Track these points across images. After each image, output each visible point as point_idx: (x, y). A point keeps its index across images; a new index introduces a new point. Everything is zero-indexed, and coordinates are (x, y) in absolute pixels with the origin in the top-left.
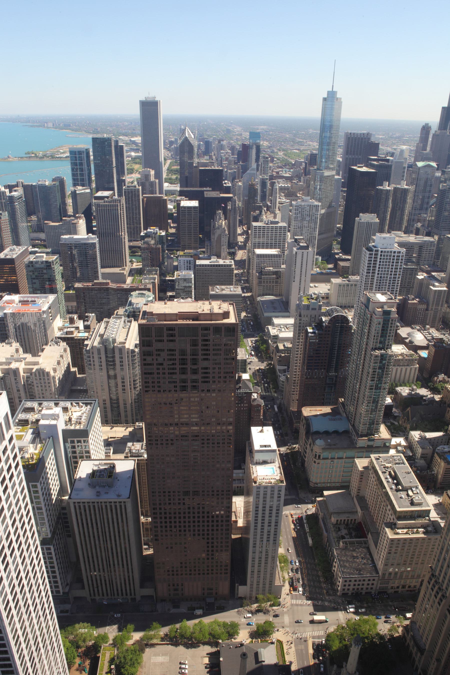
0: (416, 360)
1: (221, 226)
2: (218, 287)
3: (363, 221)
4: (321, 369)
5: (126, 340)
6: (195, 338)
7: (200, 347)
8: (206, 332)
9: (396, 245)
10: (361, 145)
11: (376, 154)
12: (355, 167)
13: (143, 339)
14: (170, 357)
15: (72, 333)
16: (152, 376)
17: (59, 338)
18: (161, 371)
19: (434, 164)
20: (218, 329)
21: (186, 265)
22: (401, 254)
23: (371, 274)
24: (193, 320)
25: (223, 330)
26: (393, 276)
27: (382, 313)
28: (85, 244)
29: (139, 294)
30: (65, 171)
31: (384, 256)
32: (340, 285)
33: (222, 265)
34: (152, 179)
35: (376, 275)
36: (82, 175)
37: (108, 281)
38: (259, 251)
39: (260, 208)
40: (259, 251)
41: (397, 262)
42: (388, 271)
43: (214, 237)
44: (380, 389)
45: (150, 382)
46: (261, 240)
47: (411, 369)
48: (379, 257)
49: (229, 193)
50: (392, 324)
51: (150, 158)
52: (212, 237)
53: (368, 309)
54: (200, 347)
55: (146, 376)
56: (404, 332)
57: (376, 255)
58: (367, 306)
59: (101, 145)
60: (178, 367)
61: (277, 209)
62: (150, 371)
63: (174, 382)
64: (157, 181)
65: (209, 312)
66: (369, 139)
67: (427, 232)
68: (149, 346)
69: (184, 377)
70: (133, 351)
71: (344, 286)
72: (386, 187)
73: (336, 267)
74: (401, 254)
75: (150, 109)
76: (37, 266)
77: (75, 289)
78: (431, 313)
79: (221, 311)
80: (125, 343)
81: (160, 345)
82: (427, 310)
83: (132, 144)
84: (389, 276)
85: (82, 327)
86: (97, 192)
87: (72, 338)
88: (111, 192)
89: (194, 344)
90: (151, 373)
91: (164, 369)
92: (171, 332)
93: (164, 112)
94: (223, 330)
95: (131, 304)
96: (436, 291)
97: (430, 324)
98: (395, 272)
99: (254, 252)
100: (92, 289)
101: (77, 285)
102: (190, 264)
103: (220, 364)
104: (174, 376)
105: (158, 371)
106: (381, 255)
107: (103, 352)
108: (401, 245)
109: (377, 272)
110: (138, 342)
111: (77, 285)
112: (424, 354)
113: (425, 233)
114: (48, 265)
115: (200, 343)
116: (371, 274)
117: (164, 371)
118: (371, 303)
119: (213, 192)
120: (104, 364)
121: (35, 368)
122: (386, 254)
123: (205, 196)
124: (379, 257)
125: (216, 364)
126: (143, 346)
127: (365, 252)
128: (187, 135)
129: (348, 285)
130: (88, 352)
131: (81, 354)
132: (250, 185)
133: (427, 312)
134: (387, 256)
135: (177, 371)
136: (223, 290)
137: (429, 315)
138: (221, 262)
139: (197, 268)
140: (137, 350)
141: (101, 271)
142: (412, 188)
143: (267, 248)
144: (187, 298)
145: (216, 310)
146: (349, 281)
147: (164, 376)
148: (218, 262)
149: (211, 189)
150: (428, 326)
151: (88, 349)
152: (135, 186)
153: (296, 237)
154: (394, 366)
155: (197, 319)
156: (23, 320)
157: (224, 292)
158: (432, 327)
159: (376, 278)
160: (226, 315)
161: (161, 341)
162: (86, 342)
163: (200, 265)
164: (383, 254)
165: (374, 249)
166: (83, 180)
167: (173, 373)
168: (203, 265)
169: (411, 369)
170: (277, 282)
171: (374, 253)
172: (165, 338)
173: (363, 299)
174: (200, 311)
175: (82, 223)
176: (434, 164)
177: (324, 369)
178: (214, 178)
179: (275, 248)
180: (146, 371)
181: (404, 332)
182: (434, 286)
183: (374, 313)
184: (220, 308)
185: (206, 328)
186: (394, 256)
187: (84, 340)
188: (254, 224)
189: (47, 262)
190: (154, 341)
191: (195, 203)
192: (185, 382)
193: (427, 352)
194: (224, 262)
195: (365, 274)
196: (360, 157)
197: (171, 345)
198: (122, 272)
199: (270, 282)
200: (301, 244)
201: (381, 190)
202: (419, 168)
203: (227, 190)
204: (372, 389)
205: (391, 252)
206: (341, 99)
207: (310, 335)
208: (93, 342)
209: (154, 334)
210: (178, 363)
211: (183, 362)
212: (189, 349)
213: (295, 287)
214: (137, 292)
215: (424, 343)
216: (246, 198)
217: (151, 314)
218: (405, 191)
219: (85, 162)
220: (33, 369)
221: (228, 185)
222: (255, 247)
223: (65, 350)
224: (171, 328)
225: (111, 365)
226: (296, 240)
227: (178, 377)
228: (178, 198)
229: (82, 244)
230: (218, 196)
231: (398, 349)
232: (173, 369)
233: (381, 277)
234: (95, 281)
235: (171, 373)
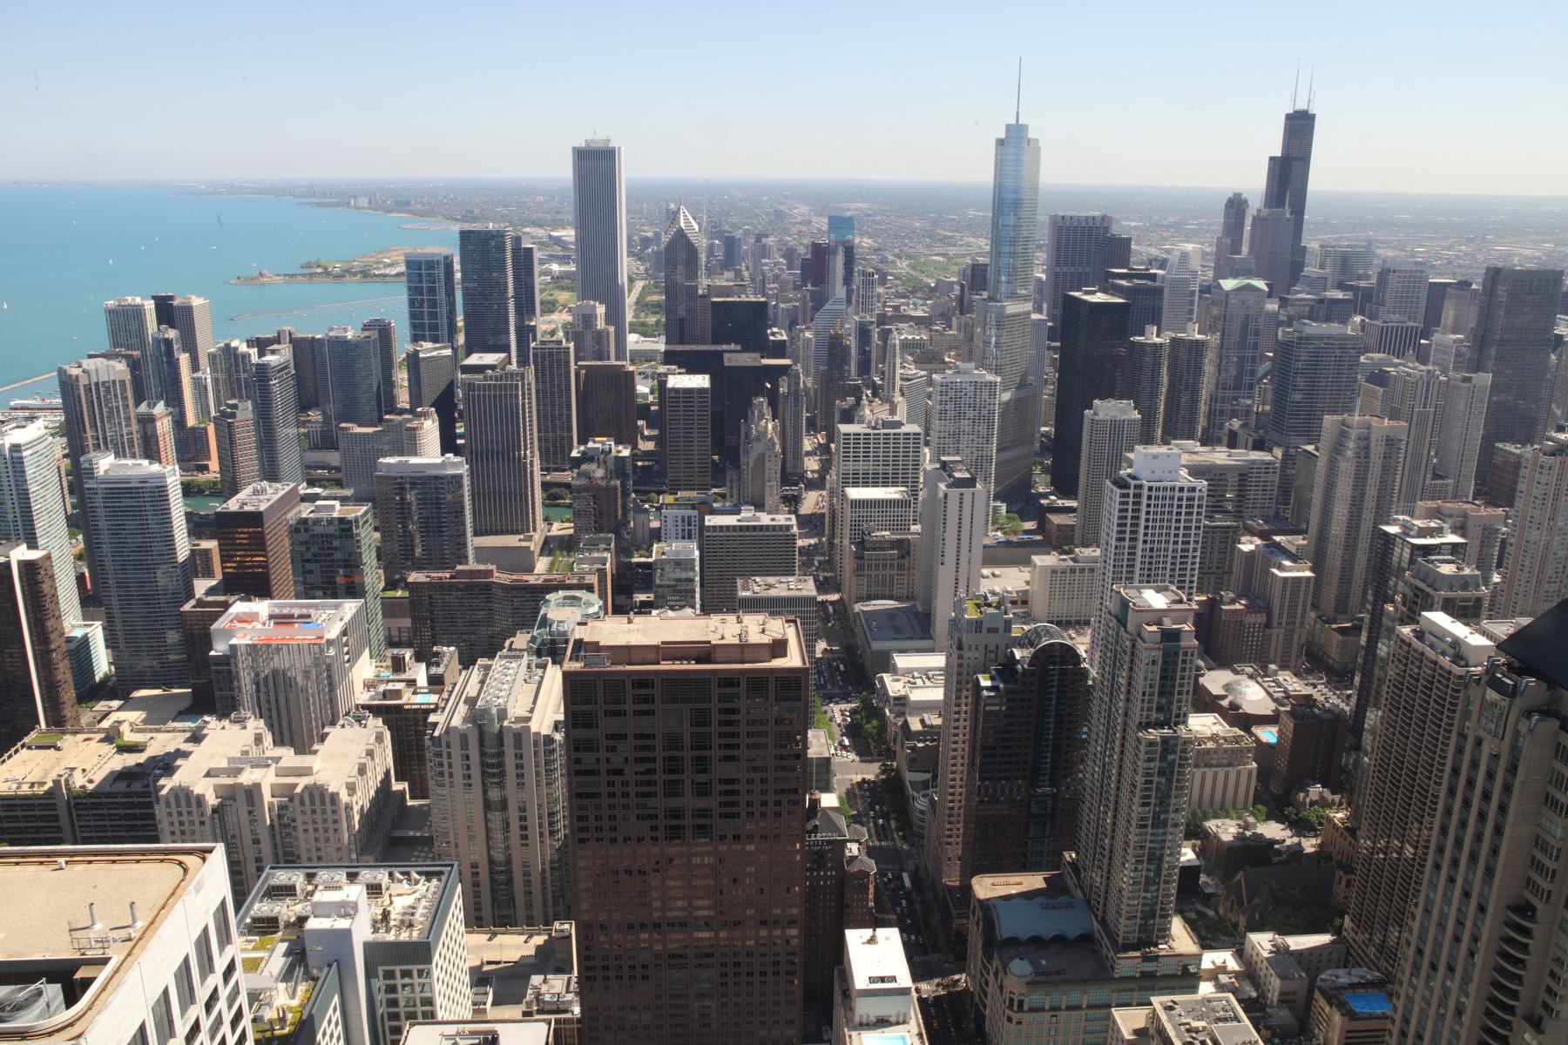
0: (1249, 750)
1: (765, 433)
3: (1101, 416)
4: (1016, 778)
5: (532, 711)
6: (701, 706)
7: (715, 729)
8: (729, 690)
9: (1184, 473)
10: (1089, 244)
11: (1125, 264)
12: (1076, 294)
13: (575, 708)
14: (641, 754)
15: (397, 694)
16: (596, 801)
17: (364, 707)
18: (618, 789)
19: (1260, 284)
20: (759, 681)
22: (1197, 494)
23: (1127, 543)
24: (698, 662)
25: (772, 684)
26: (1180, 546)
28: (436, 478)
29: (565, 598)
30: (394, 307)
31: (1157, 498)
32: (1054, 572)
33: (767, 527)
34: (600, 324)
35: (1140, 545)
36: (433, 315)
37: (493, 567)
38: (855, 493)
39: (856, 392)
40: (855, 493)
41: (1187, 514)
42: (1168, 535)
43: (748, 461)
44: (1165, 825)
45: (591, 817)
46: (861, 466)
47: (1239, 773)
49: (783, 357)
51: (596, 276)
52: (743, 459)
54: (715, 729)
55: (580, 801)
56: (1215, 681)
58: (1122, 622)
59: (482, 248)
60: (660, 777)
61: (897, 393)
62: (590, 790)
63: (651, 817)
64: (612, 329)
65: (736, 641)
66: (1107, 229)
68: (588, 725)
69: (675, 803)
70: (549, 740)
72: (1152, 337)
73: (1041, 529)
74: (1197, 494)
75: (596, 165)
76: (318, 530)
77: (407, 586)
78: (1277, 634)
79: (766, 639)
80: (529, 719)
81: (615, 725)
82: (1268, 625)
83: (553, 247)
84: (1171, 547)
85: (422, 681)
86: (468, 354)
87: (400, 707)
88: (503, 355)
89: (701, 719)
90: (592, 796)
91: (625, 784)
92: (643, 691)
93: (629, 173)
94: (772, 684)
95: (545, 622)
96: (1286, 579)
97: (1279, 659)
99: (844, 495)
100: (451, 587)
101: (414, 577)
103: (764, 769)
104: (651, 802)
105: (611, 790)
106: (1149, 498)
107: (473, 742)
108: (1196, 471)
109: (1141, 537)
110: (561, 717)
111: (414, 577)
112: (1268, 735)
114: (345, 527)
115: (715, 717)
116: (1127, 543)
117: (626, 789)
119: (745, 355)
120: (476, 772)
121: (302, 782)
123: (726, 364)
124: (1145, 501)
125: (755, 769)
126: (575, 726)
129: (1073, 571)
130: (437, 741)
131: (420, 747)
132: (831, 337)
133: (1268, 631)
134: (1164, 498)
135: (660, 789)
136: (770, 586)
137: (1274, 637)
138: (765, 519)
140: (558, 737)
141: (473, 542)
142: (1213, 339)
143: (875, 484)
144: (682, 607)
145: (755, 637)
146: (1074, 560)
147: (625, 801)
148: (758, 519)
149: (739, 347)
150: (1273, 667)
151: (436, 734)
152: (560, 342)
154: (1196, 766)
155: (708, 661)
156: (278, 662)
157: (773, 593)
158: (1283, 667)
159: (1139, 553)
160: (779, 648)
161: (618, 714)
162: (432, 718)
163: (714, 527)
164: (1153, 494)
165: (1133, 482)
166: (435, 327)
167: (649, 795)
168: (721, 527)
169: (1239, 773)
170: (900, 567)
171: (1132, 492)
172: (629, 707)
173: (1111, 604)
174: (715, 640)
175: (430, 429)
176: (1260, 284)
177: (1024, 778)
178: (745, 323)
179: (895, 484)
180: (579, 790)
181: (1215, 681)
182: (1281, 567)
183: (1139, 635)
185: (729, 680)
186: (1180, 499)
187: (427, 712)
188: (844, 428)
189: (341, 520)
190: (601, 714)
191: (701, 381)
192: (677, 817)
193: (1274, 729)
195: (1114, 543)
197: (644, 724)
198: (524, 544)
199: (885, 566)
200: (957, 475)
201: (1142, 345)
202: (1227, 294)
203: (779, 349)
204: (1145, 826)
205: (1173, 489)
206: (1037, 141)
207: (985, 693)
208: (451, 718)
209: (600, 698)
210: (660, 770)
211: (674, 766)
212: (687, 731)
213: (945, 576)
214: (561, 593)
215: (1267, 708)
217: (595, 646)
218: (1198, 346)
220: (296, 785)
221: (779, 338)
222: (846, 484)
223: (379, 738)
224: (643, 681)
225: (494, 775)
226: (944, 465)
227: (659, 804)
228: (662, 369)
229: (429, 477)
230: (757, 364)
231: (1202, 725)
232: (649, 783)
233: (1152, 550)
234: (459, 567)
235: (644, 795)
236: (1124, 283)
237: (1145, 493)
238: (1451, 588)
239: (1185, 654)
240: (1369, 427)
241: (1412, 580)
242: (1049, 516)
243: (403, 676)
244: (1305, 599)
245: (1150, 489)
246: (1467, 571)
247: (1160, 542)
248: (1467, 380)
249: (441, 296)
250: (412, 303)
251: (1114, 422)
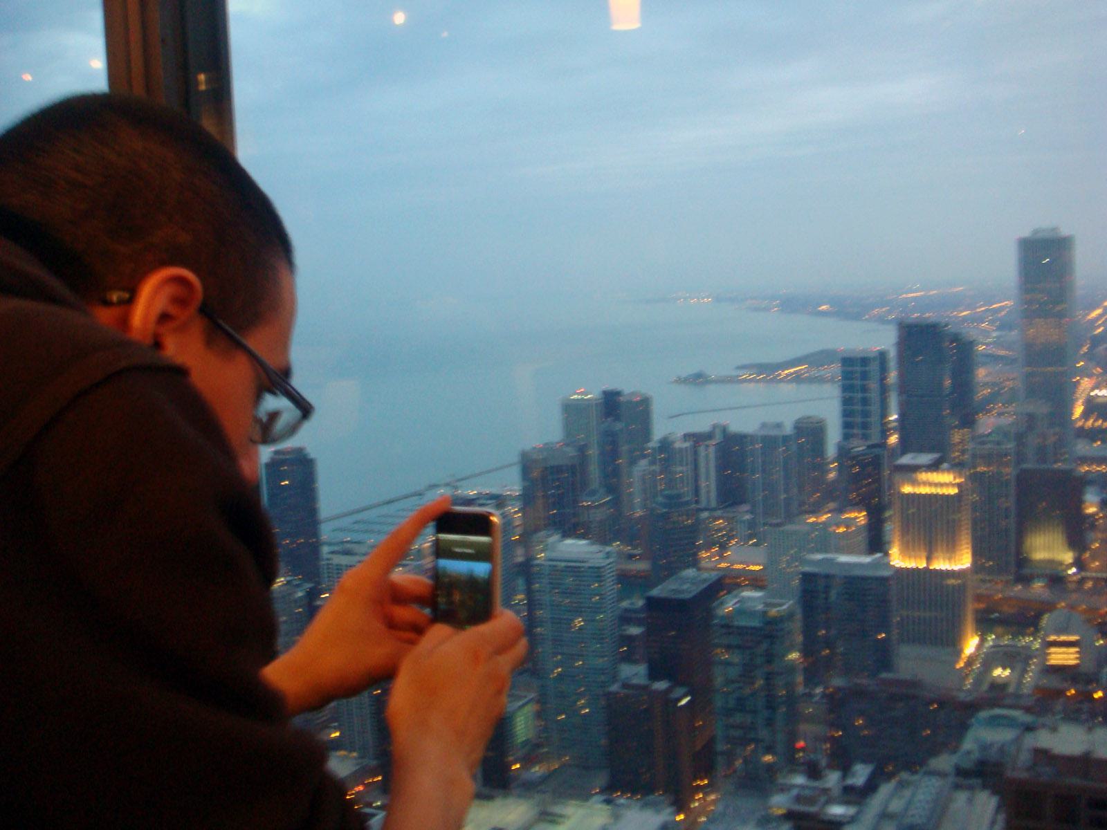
15: (811, 801)
28: (864, 579)
30: (825, 405)
36: (866, 414)
77: (1099, 326)
85: (836, 792)
86: (904, 453)
152: (998, 443)
166: (865, 426)
219: (874, 385)
234: (884, 675)
243: (816, 784)
249: (874, 395)
250: (846, 402)
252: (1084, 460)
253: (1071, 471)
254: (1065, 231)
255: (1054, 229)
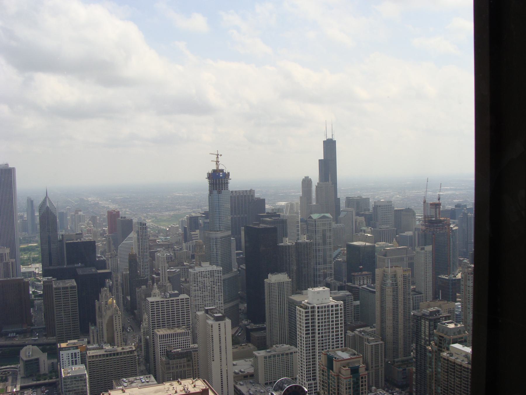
2: (125, 379)
10: (248, 203)
19: (328, 215)
21: (71, 360)
22: (339, 308)
27: (349, 372)
32: (265, 357)
33: (121, 353)
35: (317, 335)
38: (161, 332)
41: (336, 317)
48: (317, 314)
49: (105, 268)
50: (362, 382)
52: (98, 320)
53: (332, 370)
57: (313, 312)
61: (167, 281)
65: (184, 393)
66: (253, 196)
67: (338, 287)
71: (270, 357)
72: (287, 242)
74: (339, 308)
79: (197, 390)
84: (331, 334)
96: (372, 346)
98: (336, 328)
102: (76, 357)
106: (318, 312)
109: (317, 332)
113: (337, 288)
118: (334, 362)
122: (323, 309)
124: (317, 314)
127: (300, 311)
128: (48, 205)
139: (87, 360)
153: (206, 308)
158: (378, 387)
164: (320, 310)
171: (310, 310)
176: (328, 215)
183: (340, 372)
184: (195, 386)
188: (150, 299)
194: (123, 349)
195: (305, 336)
196: (246, 215)
199: (181, 367)
200: (216, 315)
201: (282, 246)
203: (103, 265)
205: (328, 306)
216: (124, 273)
226: (207, 311)
228: (45, 279)
233: (322, 337)
236: (268, 219)
237: (316, 310)
238: (454, 334)
239: (362, 378)
240: (395, 272)
241: (438, 333)
242: (251, 333)
244: (381, 355)
245: (318, 308)
246: (459, 326)
247: (325, 333)
248: (423, 249)
251: (279, 284)
252: (24, 273)
253: (22, 279)
254: (11, 166)
255: (7, 165)
